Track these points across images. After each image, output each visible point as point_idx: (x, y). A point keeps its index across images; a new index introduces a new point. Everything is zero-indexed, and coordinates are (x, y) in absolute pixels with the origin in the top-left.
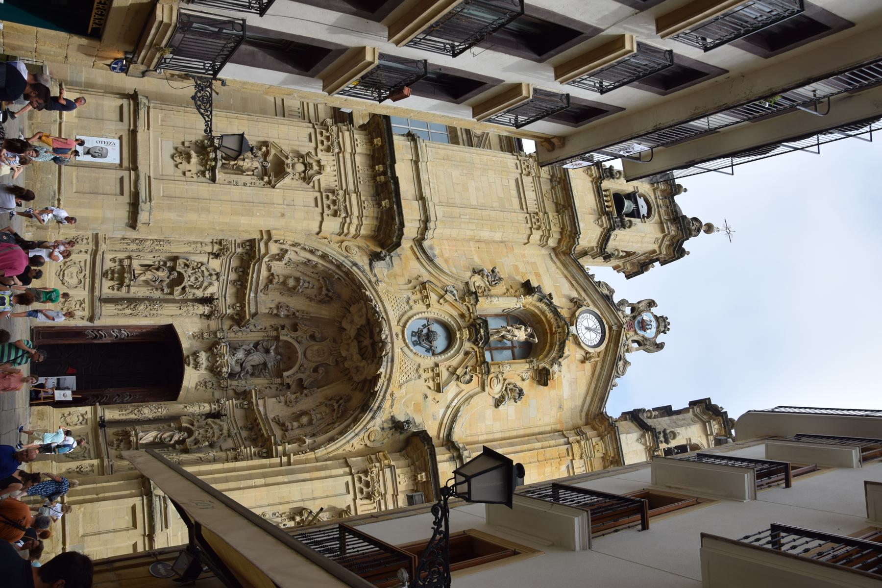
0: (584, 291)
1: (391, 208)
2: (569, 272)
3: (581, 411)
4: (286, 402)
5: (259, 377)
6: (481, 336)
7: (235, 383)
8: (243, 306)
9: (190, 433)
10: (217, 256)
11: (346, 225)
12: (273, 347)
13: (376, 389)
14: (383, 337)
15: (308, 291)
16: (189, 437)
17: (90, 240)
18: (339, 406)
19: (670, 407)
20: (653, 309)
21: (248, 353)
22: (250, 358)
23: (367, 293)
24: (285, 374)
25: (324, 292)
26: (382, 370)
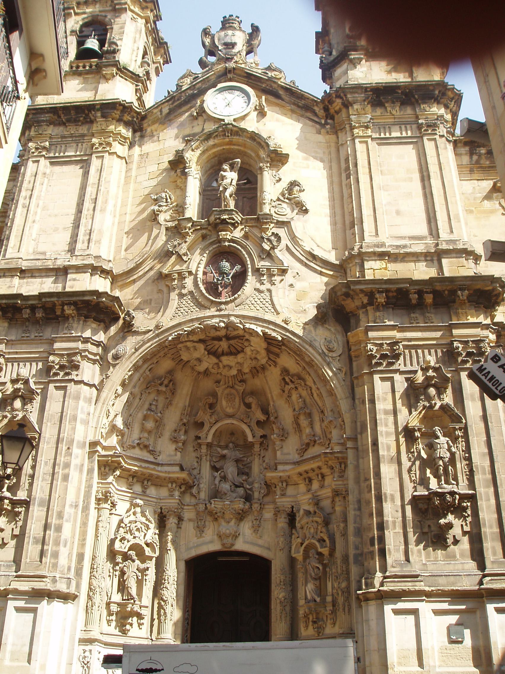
1: (75, 304)
5: (250, 468)
6: (229, 219)
7: (256, 495)
8: (172, 481)
10: (113, 505)
11: (91, 356)
12: (219, 449)
13: (280, 339)
15: (160, 406)
16: (315, 548)
17: (87, 648)
19: (317, 33)
20: (213, 31)
21: (224, 478)
22: (230, 476)
23: (170, 338)
24: (250, 439)
25: (163, 388)
26: (259, 330)
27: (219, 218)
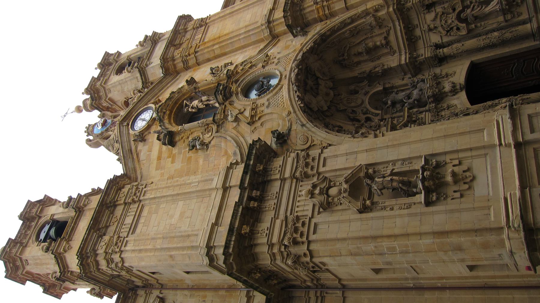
0: (131, 150)
2: (134, 165)
3: (178, 79)
4: (383, 66)
9: (459, 18)
14: (296, 71)
18: (343, 55)
27: (221, 92)
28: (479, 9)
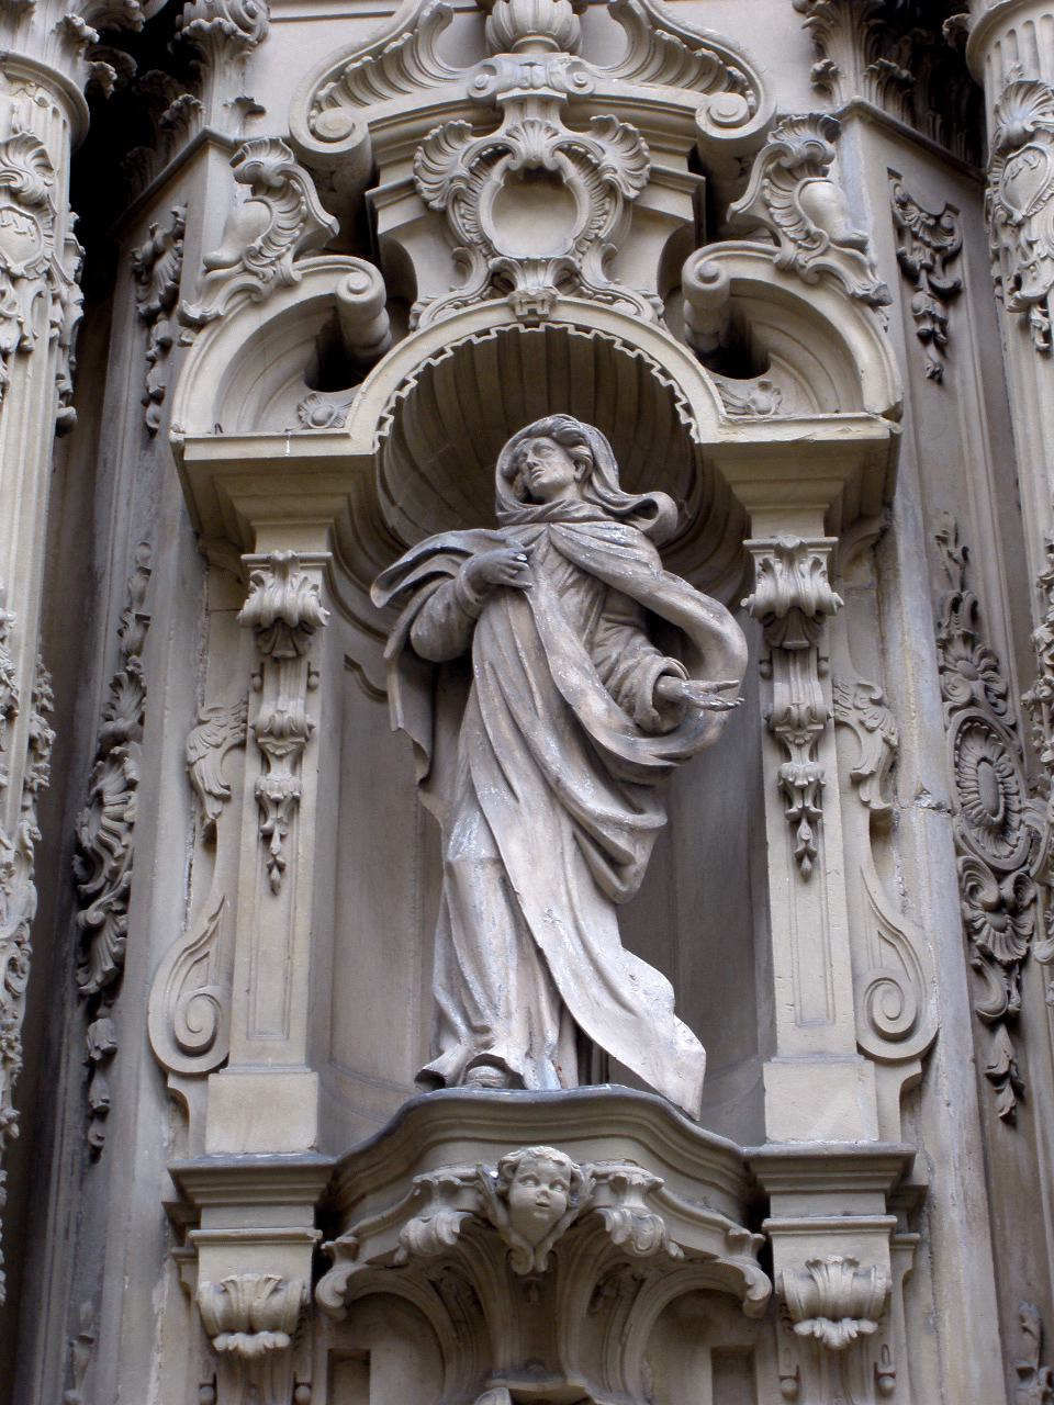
28: (596, 709)
